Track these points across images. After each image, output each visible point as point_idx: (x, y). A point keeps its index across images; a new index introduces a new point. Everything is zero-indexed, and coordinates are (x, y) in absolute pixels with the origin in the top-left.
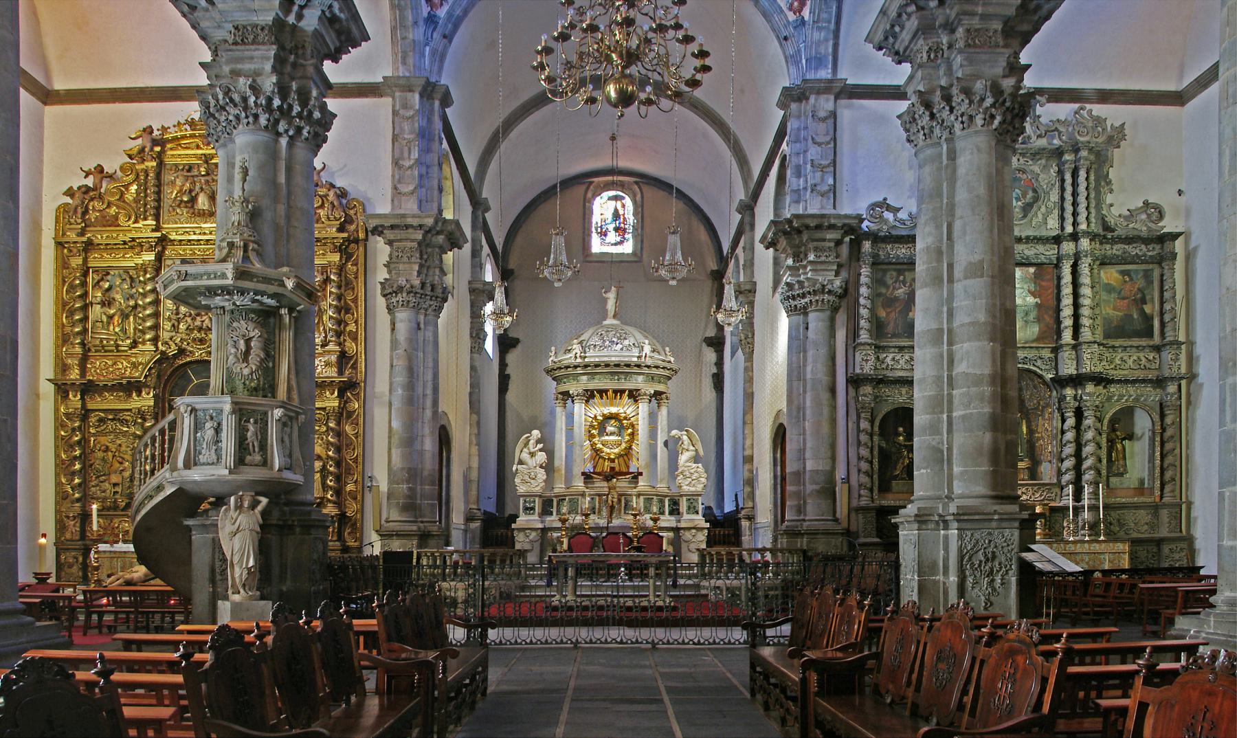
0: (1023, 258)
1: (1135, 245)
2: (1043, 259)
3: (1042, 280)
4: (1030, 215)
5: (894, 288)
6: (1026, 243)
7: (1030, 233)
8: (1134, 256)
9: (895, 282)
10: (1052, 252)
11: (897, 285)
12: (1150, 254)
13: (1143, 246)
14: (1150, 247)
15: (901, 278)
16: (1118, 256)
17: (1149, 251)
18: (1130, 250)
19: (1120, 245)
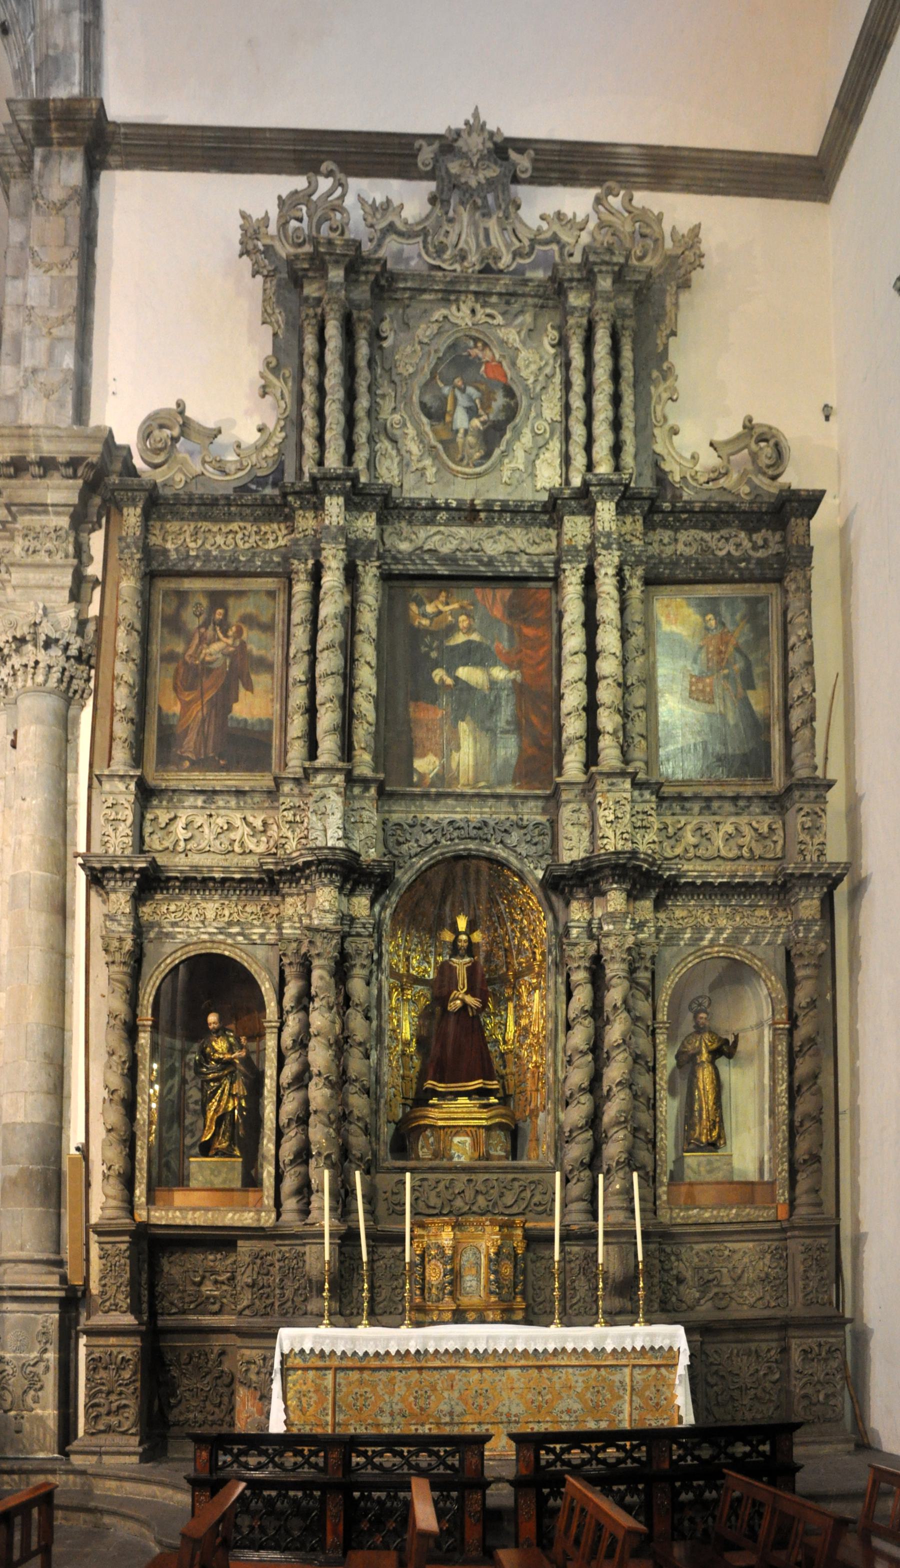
0: (480, 561)
1: (724, 532)
2: (524, 565)
3: (526, 622)
4: (497, 452)
5: (202, 639)
6: (489, 523)
7: (499, 494)
8: (722, 559)
9: (205, 625)
10: (545, 547)
11: (210, 632)
12: (761, 554)
13: (743, 534)
14: (758, 538)
15: (219, 614)
16: (688, 559)
17: (755, 548)
18: (713, 545)
19: (693, 532)
